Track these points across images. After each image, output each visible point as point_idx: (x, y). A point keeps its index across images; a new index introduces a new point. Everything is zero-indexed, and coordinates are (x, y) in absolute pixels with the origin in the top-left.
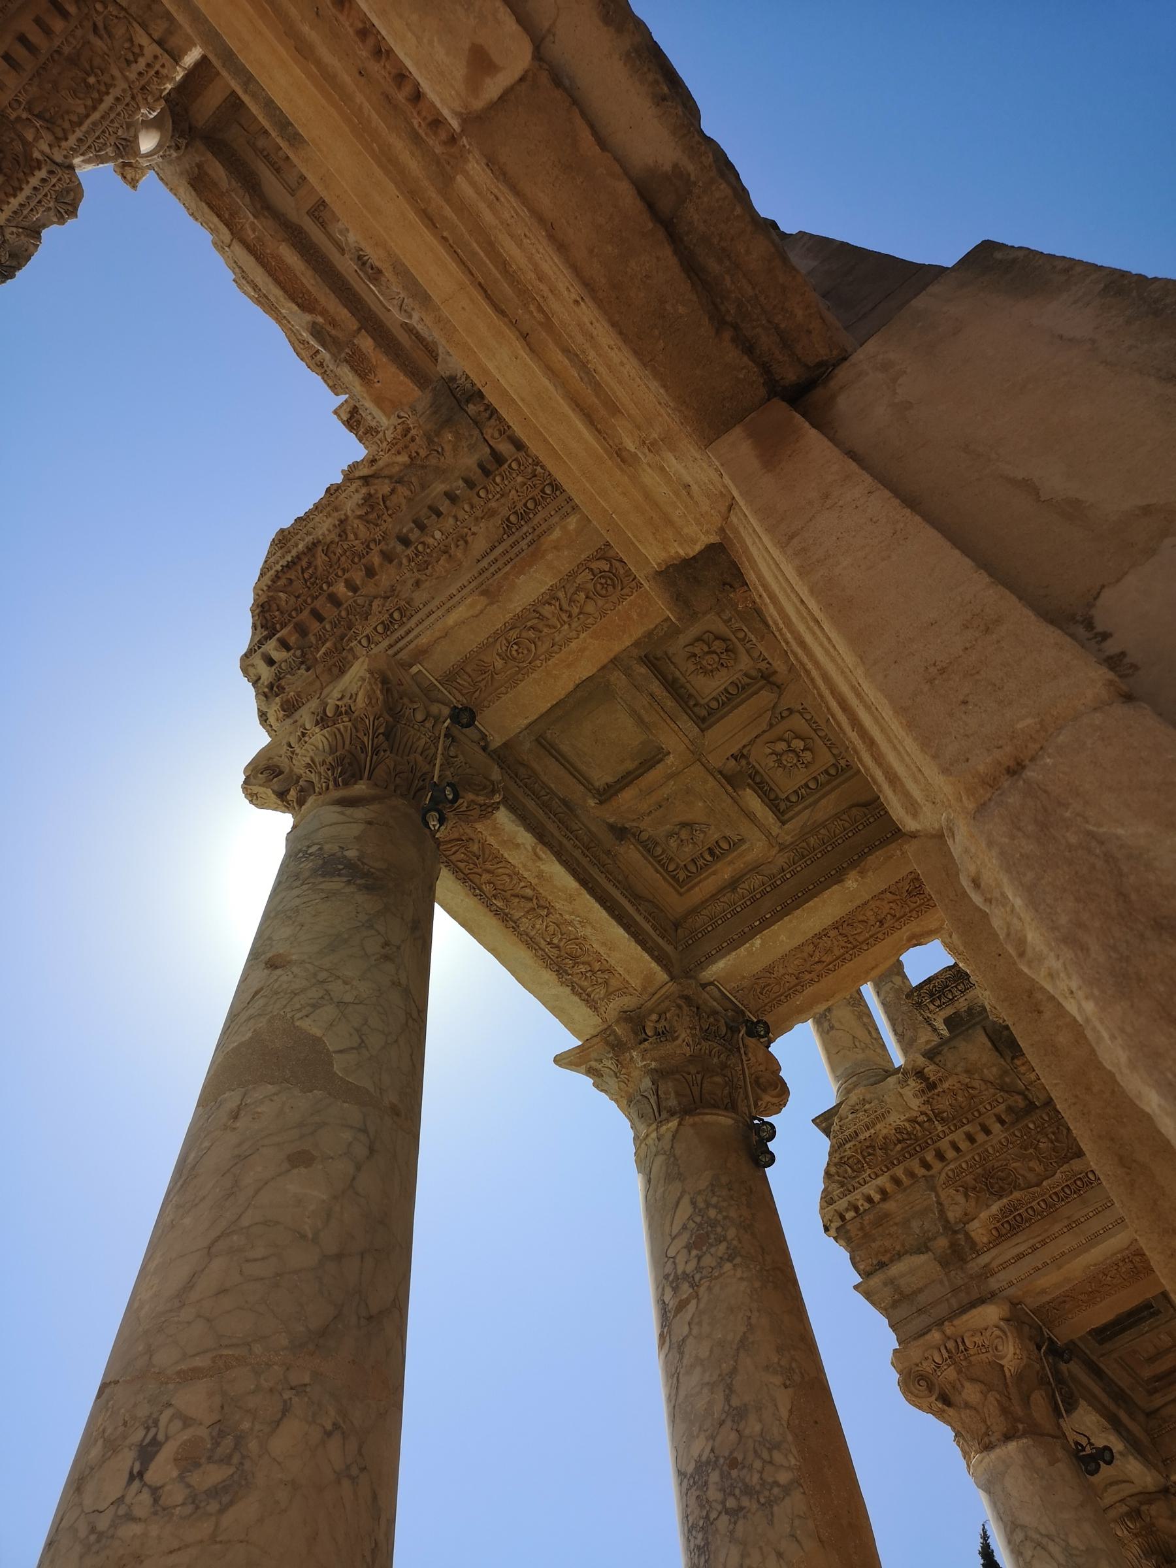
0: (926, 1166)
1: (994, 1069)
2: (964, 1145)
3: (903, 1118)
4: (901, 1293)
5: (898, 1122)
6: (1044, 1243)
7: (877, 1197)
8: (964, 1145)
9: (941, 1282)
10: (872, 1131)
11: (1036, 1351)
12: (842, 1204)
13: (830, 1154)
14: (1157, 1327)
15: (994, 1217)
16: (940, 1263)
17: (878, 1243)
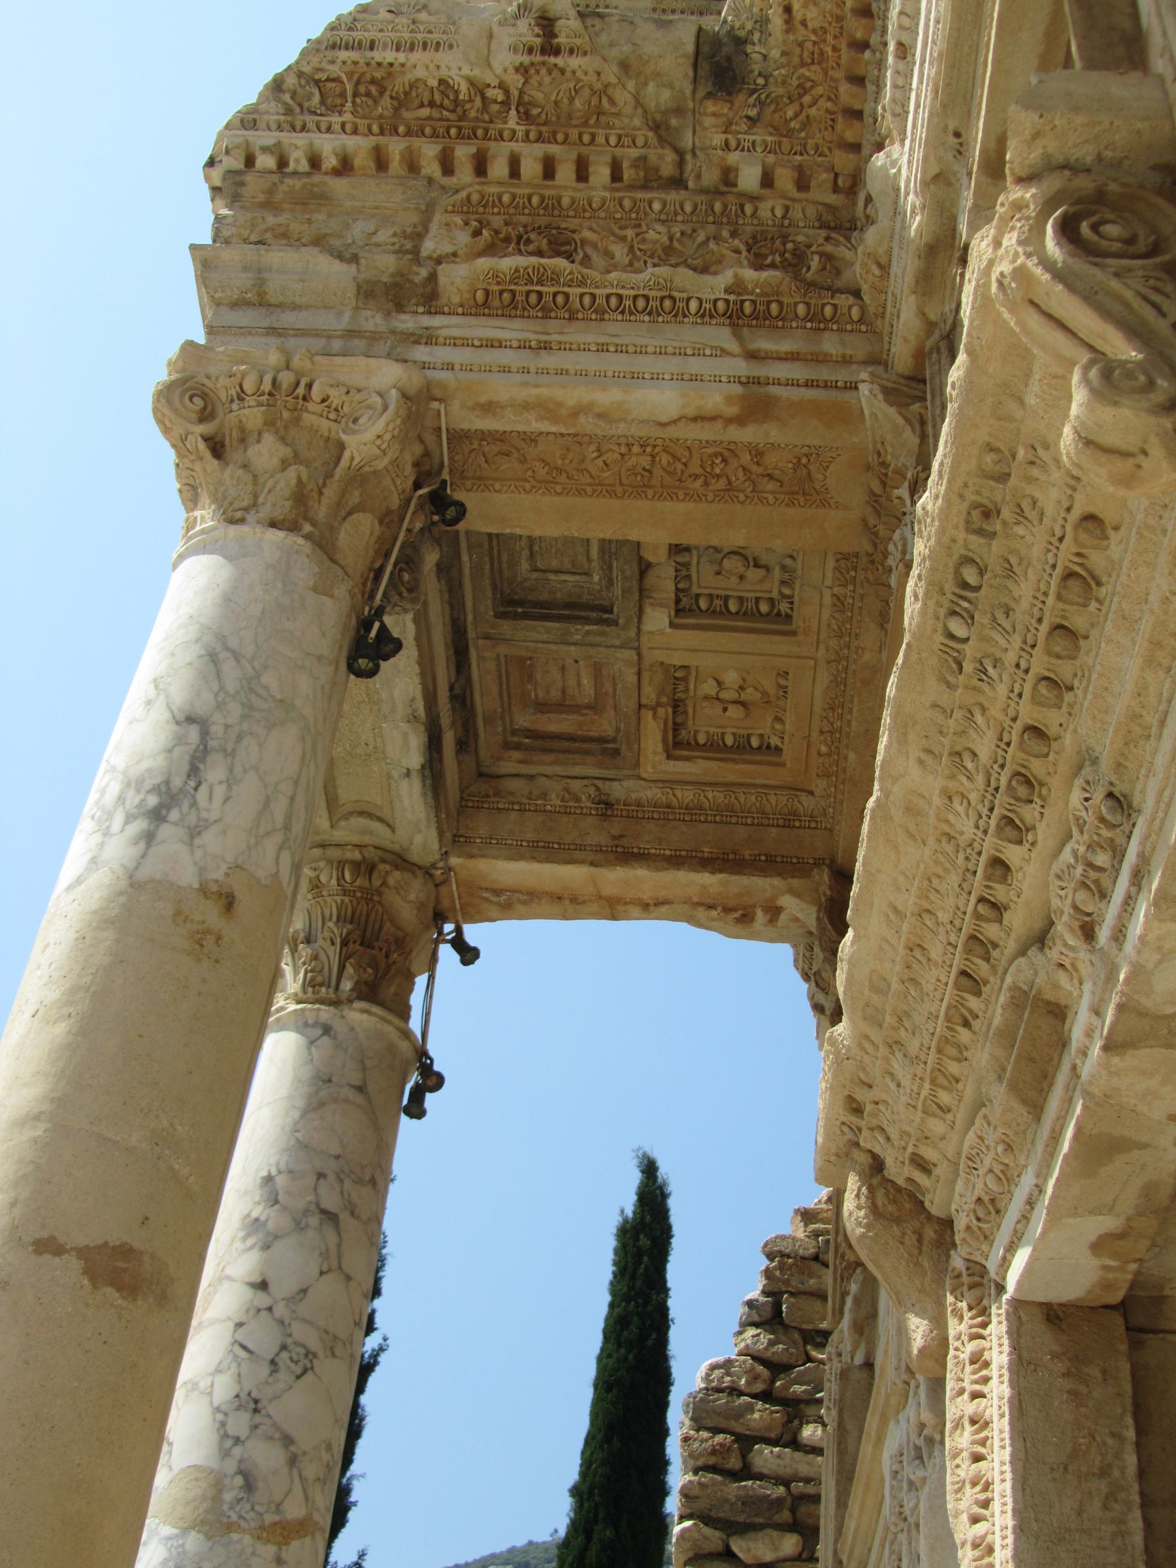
0: (448, 167)
1: (666, 95)
2: (530, 168)
3: (466, 71)
4: (262, 295)
5: (454, 73)
6: (545, 347)
7: (330, 162)
8: (530, 168)
9: (340, 314)
10: (401, 57)
11: (409, 483)
12: (262, 138)
13: (304, 53)
14: (594, 645)
15: (496, 276)
16: (359, 287)
17: (282, 219)
